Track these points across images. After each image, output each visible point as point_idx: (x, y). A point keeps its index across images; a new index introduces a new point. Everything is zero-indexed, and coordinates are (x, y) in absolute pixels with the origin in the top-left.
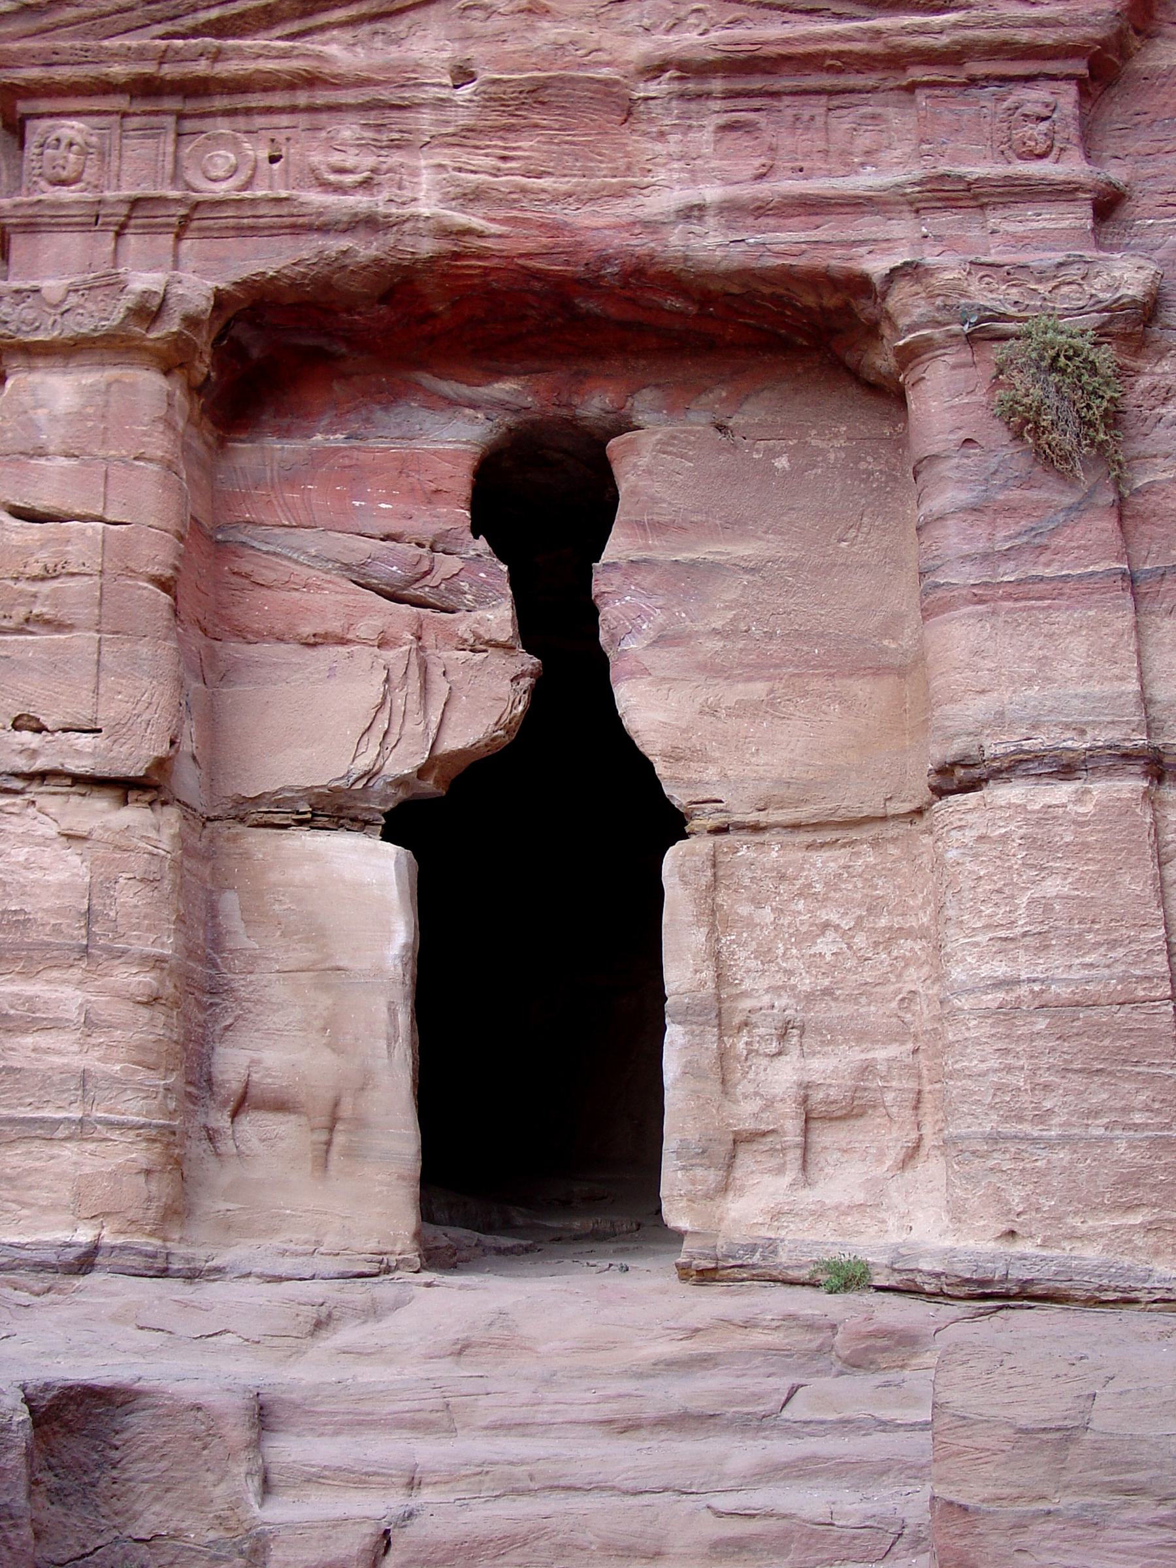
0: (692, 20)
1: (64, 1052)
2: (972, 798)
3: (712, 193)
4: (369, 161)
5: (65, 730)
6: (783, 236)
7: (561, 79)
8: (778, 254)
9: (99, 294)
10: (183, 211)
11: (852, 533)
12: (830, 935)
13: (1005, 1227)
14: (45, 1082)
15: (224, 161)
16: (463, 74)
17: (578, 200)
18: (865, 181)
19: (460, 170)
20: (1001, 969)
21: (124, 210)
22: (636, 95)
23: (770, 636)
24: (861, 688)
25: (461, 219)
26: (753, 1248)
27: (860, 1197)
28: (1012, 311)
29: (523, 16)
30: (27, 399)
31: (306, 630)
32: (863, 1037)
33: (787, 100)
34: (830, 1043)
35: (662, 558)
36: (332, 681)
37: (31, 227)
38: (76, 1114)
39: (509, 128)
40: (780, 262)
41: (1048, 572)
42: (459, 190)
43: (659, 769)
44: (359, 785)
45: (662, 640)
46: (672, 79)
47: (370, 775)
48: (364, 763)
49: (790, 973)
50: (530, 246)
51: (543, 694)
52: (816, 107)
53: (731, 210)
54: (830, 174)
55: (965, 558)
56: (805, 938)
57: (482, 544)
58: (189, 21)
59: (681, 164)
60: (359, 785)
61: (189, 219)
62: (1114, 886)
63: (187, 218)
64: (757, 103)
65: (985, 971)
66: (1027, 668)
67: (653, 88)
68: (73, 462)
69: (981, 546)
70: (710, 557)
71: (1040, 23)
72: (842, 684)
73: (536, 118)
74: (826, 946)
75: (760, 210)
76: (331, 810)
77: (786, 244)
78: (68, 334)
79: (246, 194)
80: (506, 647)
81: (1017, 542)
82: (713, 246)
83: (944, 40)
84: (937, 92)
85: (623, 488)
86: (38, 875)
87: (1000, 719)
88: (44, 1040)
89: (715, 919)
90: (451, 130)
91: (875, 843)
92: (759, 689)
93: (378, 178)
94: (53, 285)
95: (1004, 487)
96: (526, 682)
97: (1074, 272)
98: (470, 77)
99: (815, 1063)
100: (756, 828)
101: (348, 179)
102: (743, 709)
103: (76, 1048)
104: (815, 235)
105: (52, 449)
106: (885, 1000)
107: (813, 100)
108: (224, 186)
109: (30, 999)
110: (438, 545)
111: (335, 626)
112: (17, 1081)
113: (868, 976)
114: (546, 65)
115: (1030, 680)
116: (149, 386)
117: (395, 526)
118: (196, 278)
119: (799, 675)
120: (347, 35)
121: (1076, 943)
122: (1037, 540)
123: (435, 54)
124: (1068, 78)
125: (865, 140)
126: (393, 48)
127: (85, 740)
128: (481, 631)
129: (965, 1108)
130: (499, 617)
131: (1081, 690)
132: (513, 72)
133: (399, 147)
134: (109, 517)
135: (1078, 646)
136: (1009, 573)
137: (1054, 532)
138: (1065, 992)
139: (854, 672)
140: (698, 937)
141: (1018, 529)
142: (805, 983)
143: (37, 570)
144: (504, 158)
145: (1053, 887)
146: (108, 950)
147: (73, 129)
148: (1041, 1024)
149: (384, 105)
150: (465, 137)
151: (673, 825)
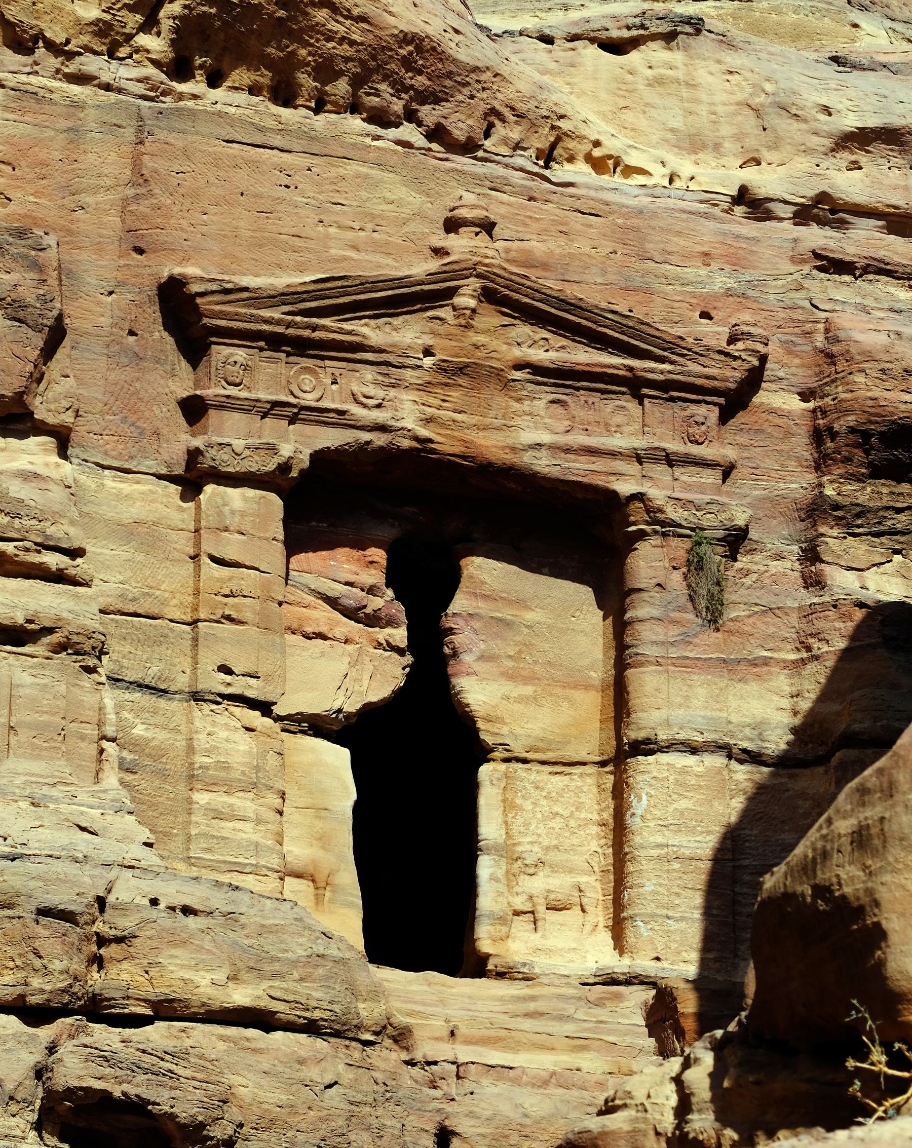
0: (542, 343)
1: (247, 832)
2: (651, 758)
3: (546, 438)
4: (381, 393)
5: (243, 675)
6: (578, 465)
7: (474, 363)
8: (574, 474)
9: (262, 452)
10: (296, 410)
11: (577, 614)
12: (558, 819)
13: (655, 955)
14: (239, 846)
15: (314, 384)
16: (428, 352)
17: (478, 429)
18: (617, 442)
19: (423, 404)
20: (660, 839)
21: (269, 406)
22: (510, 377)
23: (536, 662)
24: (578, 695)
25: (424, 432)
26: (524, 965)
27: (574, 945)
28: (684, 523)
29: (462, 328)
30: (219, 501)
31: (309, 630)
32: (571, 871)
33: (582, 392)
34: (556, 872)
35: (484, 614)
36: (323, 659)
37: (220, 407)
38: (254, 862)
39: (446, 385)
40: (575, 478)
41: (691, 655)
42: (424, 416)
43: (480, 724)
44: (334, 716)
45: (481, 658)
46: (528, 373)
47: (340, 711)
48: (336, 706)
49: (539, 835)
50: (455, 450)
51: (414, 676)
52: (595, 397)
53: (554, 448)
54: (600, 435)
55: (655, 643)
56: (545, 819)
57: (390, 593)
58: (302, 306)
59: (529, 418)
60: (334, 716)
61: (297, 414)
62: (711, 806)
63: (296, 414)
64: (568, 391)
65: (652, 839)
66: (679, 700)
67: (518, 375)
68: (242, 537)
69: (661, 638)
70: (509, 617)
71: (707, 377)
72: (570, 692)
73: (460, 381)
74: (557, 824)
75: (568, 450)
76: (317, 726)
77: (579, 469)
78: (244, 470)
79: (321, 404)
80: (401, 652)
81: (678, 638)
82: (543, 464)
83: (662, 377)
84: (654, 401)
85: (465, 573)
86: (233, 745)
87: (668, 724)
88: (239, 825)
89: (508, 806)
90: (419, 382)
91: (581, 775)
92: (528, 690)
93: (385, 403)
94: (239, 444)
95: (674, 610)
96: (408, 670)
97: (714, 508)
98: (432, 355)
99: (550, 880)
100: (525, 761)
101: (371, 402)
102: (521, 699)
103: (252, 831)
104: (593, 467)
105: (232, 528)
106: (582, 854)
107: (595, 394)
108: (309, 396)
109: (231, 805)
110: (372, 590)
111: (324, 629)
112: (226, 844)
113: (575, 841)
114: (469, 355)
115: (680, 706)
116: (275, 502)
117: (352, 578)
118: (297, 445)
119: (549, 685)
120: (372, 322)
121: (692, 831)
122: (687, 639)
123: (416, 340)
124: (715, 404)
125: (618, 419)
126: (394, 333)
127: (252, 681)
128: (391, 640)
129: (639, 901)
130: (400, 635)
131: (702, 713)
132: (453, 356)
133: (393, 387)
134: (261, 569)
135: (702, 692)
136: (674, 653)
137: (695, 635)
138: (687, 852)
139: (575, 687)
140: (498, 814)
141: (679, 632)
142: (546, 843)
143: (228, 592)
144: (444, 400)
145: (683, 804)
146: (266, 785)
147: (241, 354)
148: (676, 866)
149: (386, 362)
150: (426, 387)
151: (483, 753)
